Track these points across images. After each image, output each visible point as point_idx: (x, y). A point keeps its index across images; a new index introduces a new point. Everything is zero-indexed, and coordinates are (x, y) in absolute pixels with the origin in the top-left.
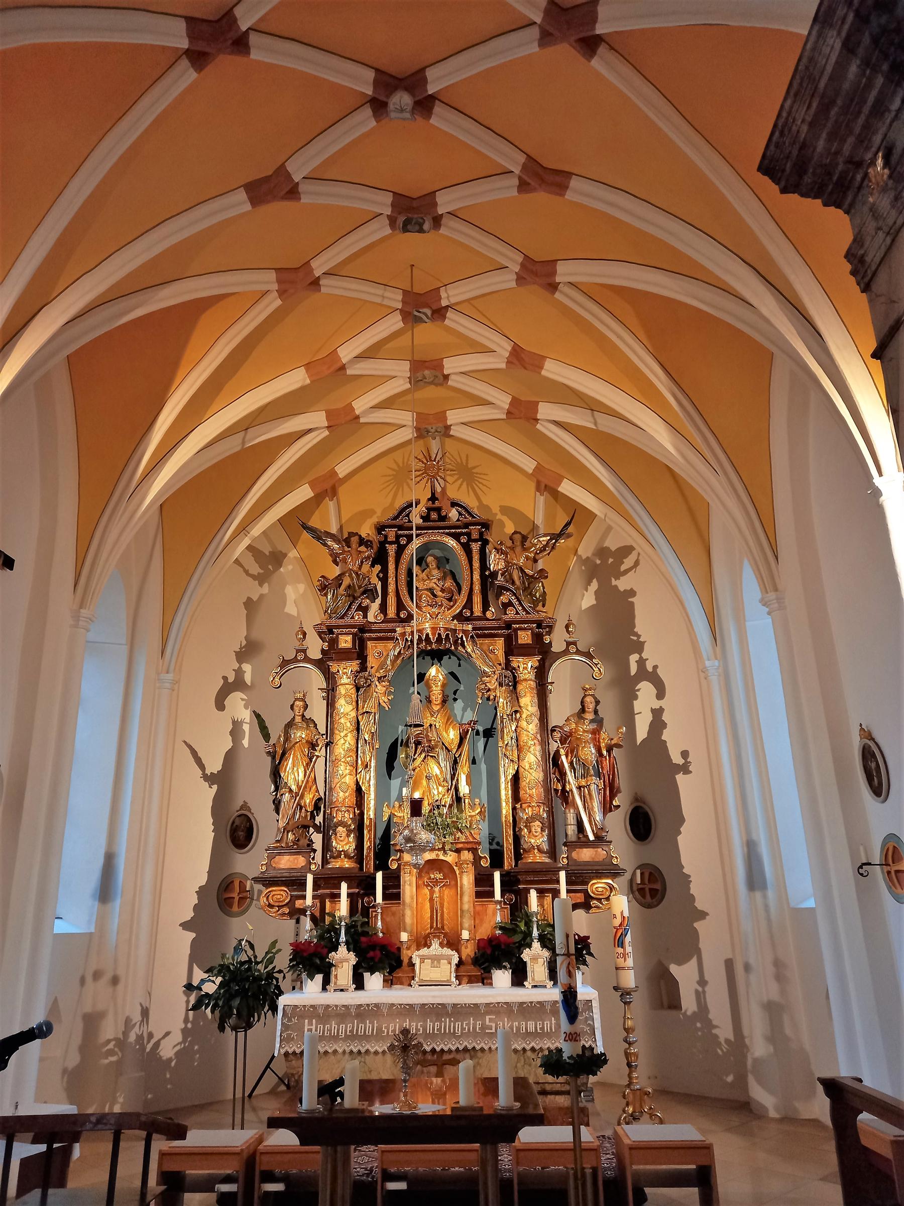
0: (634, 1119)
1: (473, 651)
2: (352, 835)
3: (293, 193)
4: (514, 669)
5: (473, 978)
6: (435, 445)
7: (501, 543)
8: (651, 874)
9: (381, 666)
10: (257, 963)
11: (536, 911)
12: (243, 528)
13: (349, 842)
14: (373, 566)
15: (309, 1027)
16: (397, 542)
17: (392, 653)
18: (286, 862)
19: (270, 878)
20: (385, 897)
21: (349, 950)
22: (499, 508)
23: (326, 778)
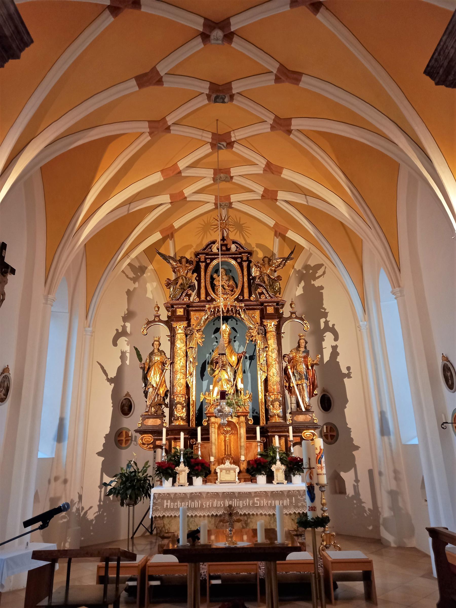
0: (326, 548)
1: (245, 317)
2: (185, 409)
3: (160, 82)
4: (265, 325)
5: (246, 479)
6: (224, 212)
7: (258, 263)
8: (331, 427)
9: (199, 324)
10: (139, 472)
11: (278, 446)
12: (127, 254)
13: (183, 412)
14: (193, 273)
15: (167, 504)
16: (205, 261)
17: (203, 318)
18: (151, 422)
19: (143, 430)
20: (202, 439)
21: (185, 466)
22: (255, 245)
23: (171, 380)
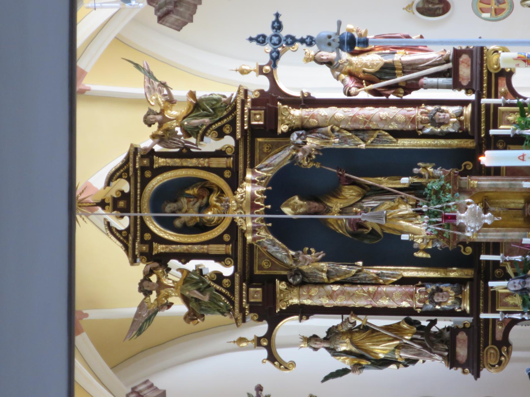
16: (150, 243)
